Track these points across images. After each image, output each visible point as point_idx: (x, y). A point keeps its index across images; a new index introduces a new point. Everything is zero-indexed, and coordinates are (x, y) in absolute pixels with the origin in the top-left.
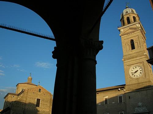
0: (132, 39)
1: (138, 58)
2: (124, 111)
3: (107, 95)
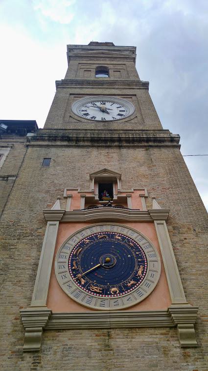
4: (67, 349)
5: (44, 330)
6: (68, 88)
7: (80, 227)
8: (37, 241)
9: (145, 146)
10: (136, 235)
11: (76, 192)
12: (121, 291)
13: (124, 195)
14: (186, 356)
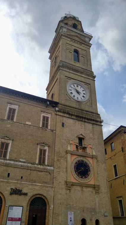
0: (78, 49)
1: (83, 76)
2: (49, 147)
3: (16, 102)
4: (75, 190)
5: (71, 185)
6: (64, 71)
7: (75, 157)
8: (65, 159)
9: (92, 123)
10: (89, 162)
11: (73, 142)
12: (85, 178)
13: (86, 146)
14: (96, 194)
